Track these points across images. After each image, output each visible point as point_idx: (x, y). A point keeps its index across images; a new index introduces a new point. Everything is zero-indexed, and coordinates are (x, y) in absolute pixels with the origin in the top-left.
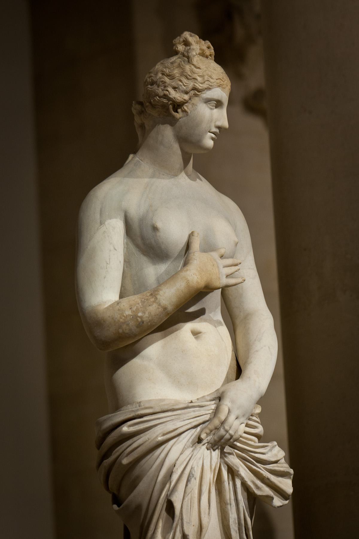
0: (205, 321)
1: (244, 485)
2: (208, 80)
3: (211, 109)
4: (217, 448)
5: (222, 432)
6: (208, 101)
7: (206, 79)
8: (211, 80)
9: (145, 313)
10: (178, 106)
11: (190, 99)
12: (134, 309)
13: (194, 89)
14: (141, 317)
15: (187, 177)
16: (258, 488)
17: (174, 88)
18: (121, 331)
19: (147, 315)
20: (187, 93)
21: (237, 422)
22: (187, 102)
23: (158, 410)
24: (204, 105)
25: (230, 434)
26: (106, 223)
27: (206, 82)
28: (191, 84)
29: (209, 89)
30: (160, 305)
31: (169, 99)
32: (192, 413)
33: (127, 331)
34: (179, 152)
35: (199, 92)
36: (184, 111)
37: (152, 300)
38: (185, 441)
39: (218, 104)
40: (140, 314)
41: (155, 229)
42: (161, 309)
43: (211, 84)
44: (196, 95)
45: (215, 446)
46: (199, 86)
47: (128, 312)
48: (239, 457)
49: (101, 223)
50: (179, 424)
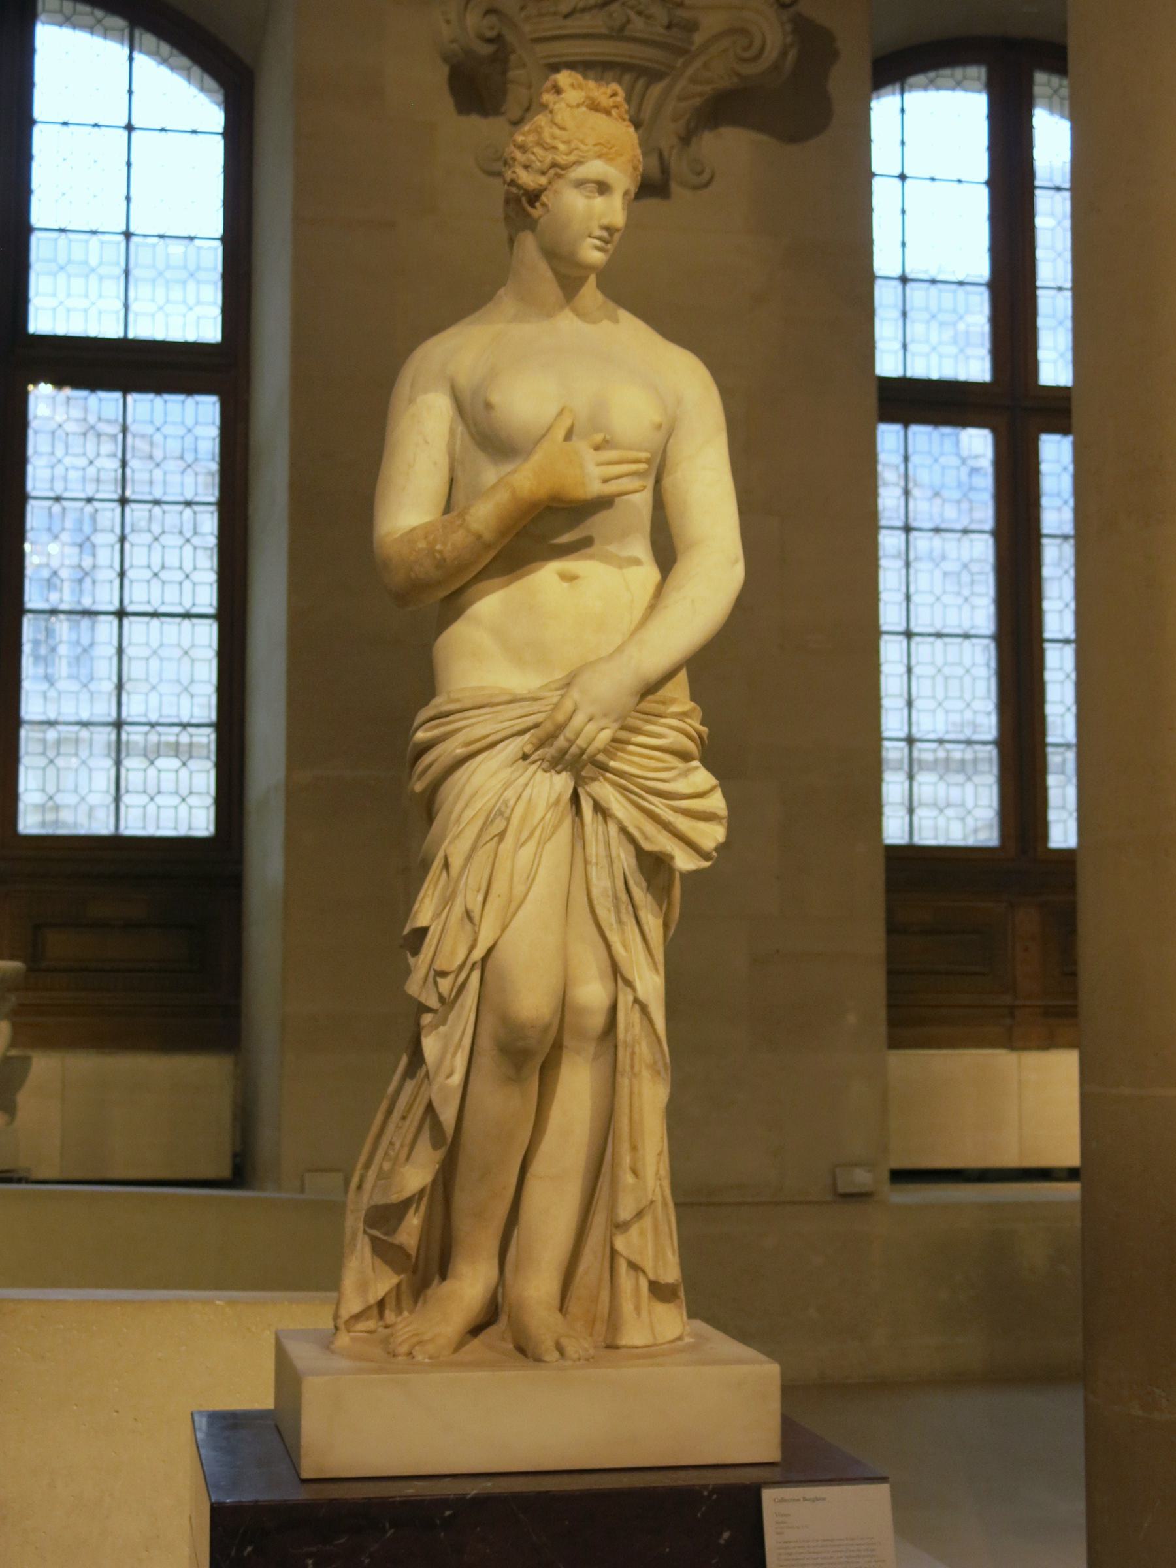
0: (591, 557)
1: (623, 830)
2: (577, 149)
3: (588, 197)
5: (561, 742)
6: (580, 184)
7: (573, 146)
8: (582, 146)
9: (444, 544)
10: (534, 197)
11: (550, 183)
12: (431, 537)
13: (554, 165)
14: (440, 552)
15: (575, 318)
16: (646, 838)
17: (526, 167)
18: (413, 575)
19: (449, 547)
20: (543, 173)
21: (591, 728)
22: (545, 189)
23: (468, 704)
25: (578, 747)
28: (549, 157)
29: (579, 163)
30: (469, 531)
31: (519, 187)
32: (518, 709)
34: (549, 274)
36: (544, 205)
37: (459, 522)
38: (503, 755)
39: (603, 188)
40: (438, 547)
41: (488, 406)
44: (558, 176)
45: (556, 765)
46: (562, 159)
47: (422, 545)
48: (614, 784)
49: (411, 401)
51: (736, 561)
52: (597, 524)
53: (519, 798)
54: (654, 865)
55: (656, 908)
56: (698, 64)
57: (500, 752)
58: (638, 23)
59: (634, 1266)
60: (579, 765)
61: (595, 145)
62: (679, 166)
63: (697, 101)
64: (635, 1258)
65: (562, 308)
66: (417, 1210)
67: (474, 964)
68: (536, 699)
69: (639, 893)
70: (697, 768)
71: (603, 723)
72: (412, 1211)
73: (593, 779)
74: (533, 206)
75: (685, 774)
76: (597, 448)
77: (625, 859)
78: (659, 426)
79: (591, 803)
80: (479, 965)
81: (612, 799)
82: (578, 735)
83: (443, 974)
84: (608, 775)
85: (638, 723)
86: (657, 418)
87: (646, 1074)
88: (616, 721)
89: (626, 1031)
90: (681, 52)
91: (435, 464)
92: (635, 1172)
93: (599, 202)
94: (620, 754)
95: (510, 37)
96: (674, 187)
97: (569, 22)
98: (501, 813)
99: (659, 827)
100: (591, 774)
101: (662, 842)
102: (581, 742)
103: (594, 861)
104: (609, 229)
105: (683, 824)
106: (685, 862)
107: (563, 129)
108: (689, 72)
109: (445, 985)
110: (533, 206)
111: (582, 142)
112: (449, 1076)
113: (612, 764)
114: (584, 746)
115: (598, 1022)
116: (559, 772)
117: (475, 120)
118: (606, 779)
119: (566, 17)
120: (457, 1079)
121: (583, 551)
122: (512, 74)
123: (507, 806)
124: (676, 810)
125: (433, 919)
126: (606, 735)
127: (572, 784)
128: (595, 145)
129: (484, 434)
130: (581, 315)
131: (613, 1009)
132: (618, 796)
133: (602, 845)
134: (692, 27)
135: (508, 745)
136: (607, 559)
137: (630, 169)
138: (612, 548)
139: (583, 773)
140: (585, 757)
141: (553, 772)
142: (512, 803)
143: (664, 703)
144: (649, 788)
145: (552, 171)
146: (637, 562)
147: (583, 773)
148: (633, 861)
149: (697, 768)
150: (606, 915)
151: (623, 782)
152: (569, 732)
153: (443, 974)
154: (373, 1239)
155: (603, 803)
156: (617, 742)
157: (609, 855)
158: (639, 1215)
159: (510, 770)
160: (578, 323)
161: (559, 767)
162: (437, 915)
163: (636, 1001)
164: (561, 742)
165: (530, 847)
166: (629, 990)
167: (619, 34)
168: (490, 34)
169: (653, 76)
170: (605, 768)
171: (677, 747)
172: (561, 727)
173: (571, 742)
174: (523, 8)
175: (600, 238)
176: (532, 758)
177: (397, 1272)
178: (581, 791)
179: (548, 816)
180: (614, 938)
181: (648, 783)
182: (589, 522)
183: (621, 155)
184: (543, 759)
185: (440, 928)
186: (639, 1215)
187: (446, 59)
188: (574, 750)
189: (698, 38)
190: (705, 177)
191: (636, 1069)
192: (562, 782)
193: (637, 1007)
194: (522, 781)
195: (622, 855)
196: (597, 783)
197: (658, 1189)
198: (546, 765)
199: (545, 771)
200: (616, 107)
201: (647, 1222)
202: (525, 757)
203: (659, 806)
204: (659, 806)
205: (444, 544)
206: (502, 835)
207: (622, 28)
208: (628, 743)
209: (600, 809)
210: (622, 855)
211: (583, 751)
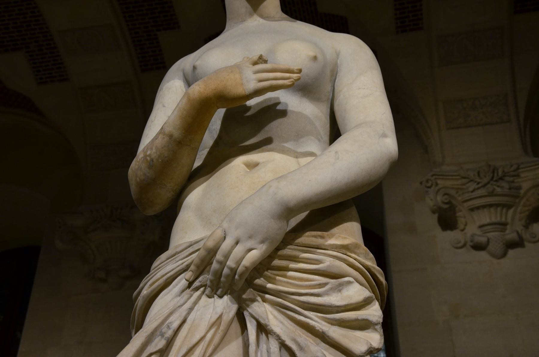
1: (283, 345)
4: (226, 293)
9: (152, 149)
14: (150, 155)
19: (154, 151)
21: (239, 250)
40: (149, 153)
42: (166, 139)
45: (217, 290)
51: (384, 136)
52: (275, 128)
56: (524, 200)
57: (174, 287)
58: (498, 190)
62: (526, 236)
63: (527, 213)
65: (251, 15)
68: (203, 239)
70: (349, 283)
73: (253, 300)
75: (338, 288)
78: (315, 58)
79: (255, 323)
81: (271, 317)
82: (227, 256)
84: (267, 296)
86: (312, 54)
88: (262, 242)
90: (517, 197)
94: (278, 278)
95: (454, 202)
96: (526, 243)
97: (473, 194)
99: (318, 340)
100: (251, 296)
102: (231, 263)
105: (336, 333)
108: (522, 203)
113: (269, 286)
116: (221, 297)
118: (264, 300)
119: (472, 192)
121: (265, 147)
123: (168, 327)
126: (254, 256)
130: (266, 18)
132: (276, 313)
134: (519, 188)
138: (289, 145)
139: (244, 296)
140: (237, 277)
141: (216, 296)
142: (176, 325)
143: (322, 237)
144: (304, 302)
147: (244, 296)
149: (349, 283)
151: (280, 300)
152: (219, 256)
155: (262, 321)
159: (178, 298)
160: (262, 21)
161: (219, 292)
164: (215, 266)
167: (492, 194)
168: (446, 201)
169: (509, 206)
170: (263, 290)
173: (222, 264)
174: (457, 193)
176: (197, 284)
178: (245, 313)
179: (209, 336)
181: (302, 298)
182: (267, 128)
184: (205, 286)
187: (434, 212)
188: (226, 271)
189: (522, 192)
192: (223, 306)
196: (256, 304)
198: (208, 290)
199: (209, 297)
203: (316, 320)
204: (316, 320)
207: (492, 192)
208: (288, 269)
211: (233, 271)
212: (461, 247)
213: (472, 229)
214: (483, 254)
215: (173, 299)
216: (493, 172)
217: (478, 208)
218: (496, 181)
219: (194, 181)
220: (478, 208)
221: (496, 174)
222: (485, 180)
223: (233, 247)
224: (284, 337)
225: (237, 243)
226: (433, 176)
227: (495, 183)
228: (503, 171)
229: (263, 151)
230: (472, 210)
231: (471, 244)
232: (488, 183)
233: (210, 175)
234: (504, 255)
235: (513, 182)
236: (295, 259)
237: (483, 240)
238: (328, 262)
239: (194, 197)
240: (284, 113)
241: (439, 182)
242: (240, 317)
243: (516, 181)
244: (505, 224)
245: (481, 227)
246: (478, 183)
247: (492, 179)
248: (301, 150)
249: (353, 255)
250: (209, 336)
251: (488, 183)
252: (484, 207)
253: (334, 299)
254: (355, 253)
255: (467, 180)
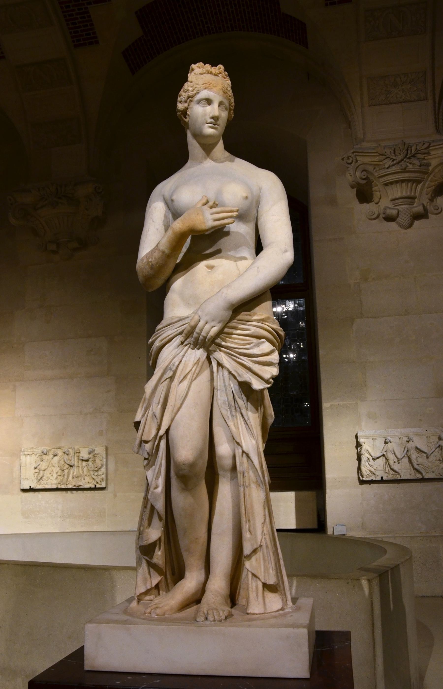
3: (204, 107)
6: (199, 102)
7: (194, 87)
8: (198, 86)
9: (152, 258)
11: (189, 105)
13: (189, 97)
14: (151, 262)
16: (239, 376)
19: (154, 260)
20: (186, 102)
21: (207, 327)
24: (198, 105)
26: (152, 206)
27: (195, 89)
29: (196, 94)
30: (159, 251)
33: (147, 274)
34: (198, 145)
35: (192, 98)
39: (209, 101)
40: (150, 260)
41: (172, 201)
42: (161, 254)
43: (198, 89)
44: (191, 101)
45: (197, 346)
46: (190, 94)
48: (225, 353)
50: (170, 332)
51: (286, 251)
52: (223, 243)
53: (181, 362)
54: (245, 387)
55: (253, 409)
56: (432, 176)
58: (410, 166)
59: (254, 575)
60: (209, 345)
61: (203, 84)
62: (430, 208)
63: (433, 187)
64: (255, 572)
65: (206, 159)
66: (160, 549)
67: (161, 437)
69: (241, 402)
70: (264, 342)
71: (213, 324)
72: (157, 548)
73: (215, 351)
74: (186, 118)
75: (258, 345)
76: (211, 207)
77: (234, 386)
78: (247, 198)
79: (216, 362)
80: (165, 437)
81: (224, 359)
82: (201, 330)
83: (146, 442)
84: (222, 349)
85: (236, 325)
86: (245, 195)
87: (253, 486)
88: (219, 322)
89: (240, 466)
90: (426, 173)
91: (157, 229)
92: (250, 531)
93: (208, 108)
94: (227, 339)
95: (371, 178)
96: (430, 215)
97: (388, 170)
98: (171, 369)
99: (248, 371)
100: (213, 349)
101: (247, 377)
102: (203, 334)
103: (219, 388)
104: (215, 119)
105: (256, 368)
106: (257, 385)
107: (192, 82)
108: (429, 179)
109: (148, 447)
110: (186, 118)
111: (198, 85)
112: (157, 487)
113: (223, 343)
114: (205, 335)
115: (228, 462)
116: (198, 349)
117: (365, 205)
118: (221, 351)
119: (387, 168)
120: (160, 489)
122: (374, 189)
123: (173, 365)
124: (259, 363)
125: (142, 418)
126: (215, 330)
127: (205, 354)
128: (203, 84)
129: (175, 213)
131: (234, 457)
132: (227, 357)
133: (222, 381)
134: (428, 165)
135: (178, 338)
136: (228, 258)
137: (221, 93)
138: (231, 253)
139: (210, 349)
140: (207, 340)
141: (196, 349)
142: (176, 364)
143: (250, 315)
145: (189, 100)
146: (245, 258)
147: (210, 349)
148: (237, 387)
149: (264, 342)
150: (227, 414)
152: (197, 330)
153: (146, 442)
154: (147, 561)
155: (220, 362)
156: (221, 333)
157: (225, 386)
158: (255, 551)
159: (177, 350)
160: (213, 163)
161: (198, 347)
162: (143, 416)
163: (243, 452)
164: (195, 335)
165: (185, 383)
166: (239, 447)
167: (404, 171)
168: (364, 177)
169: (418, 182)
170: (220, 346)
171: (256, 334)
172: (194, 328)
173: (199, 334)
174: (374, 169)
175: (211, 123)
176: (186, 343)
177: (161, 576)
178: (211, 356)
179: (194, 369)
180: (231, 423)
181: (240, 351)
182: (218, 243)
183: (216, 87)
185: (144, 421)
186: (255, 551)
187: (352, 187)
188: (201, 337)
189: (431, 168)
190: (440, 210)
191: (247, 484)
192: (200, 353)
193: (244, 455)
194: (182, 354)
195: (232, 385)
197: (263, 540)
198: (192, 346)
199: (193, 349)
200: (220, 73)
201: (259, 555)
202: (182, 343)
203: (246, 361)
204: (246, 361)
205: (152, 258)
206: (172, 378)
207: (405, 169)
208: (232, 334)
209: (220, 365)
210: (232, 385)
211: (205, 338)
212: (374, 219)
213: (385, 203)
214: (393, 225)
215: (173, 350)
216: (407, 150)
217: (391, 183)
218: (409, 158)
219: (176, 274)
220: (391, 183)
221: (409, 152)
222: (400, 157)
223: (204, 326)
224: (231, 370)
225: (206, 323)
226: (353, 153)
227: (408, 160)
228: (416, 149)
229: (216, 258)
230: (386, 185)
231: (384, 216)
232: (402, 160)
233: (185, 271)
234: (411, 225)
235: (424, 159)
236: (236, 328)
237: (394, 212)
238: (253, 330)
239: (178, 284)
240: (228, 233)
241: (359, 158)
242: (209, 359)
243: (426, 158)
244: (414, 198)
245: (392, 200)
246: (393, 160)
247: (405, 157)
248: (238, 255)
249: (266, 323)
250: (194, 369)
251: (402, 160)
252: (397, 182)
253: (256, 351)
254: (267, 322)
255: (384, 157)
